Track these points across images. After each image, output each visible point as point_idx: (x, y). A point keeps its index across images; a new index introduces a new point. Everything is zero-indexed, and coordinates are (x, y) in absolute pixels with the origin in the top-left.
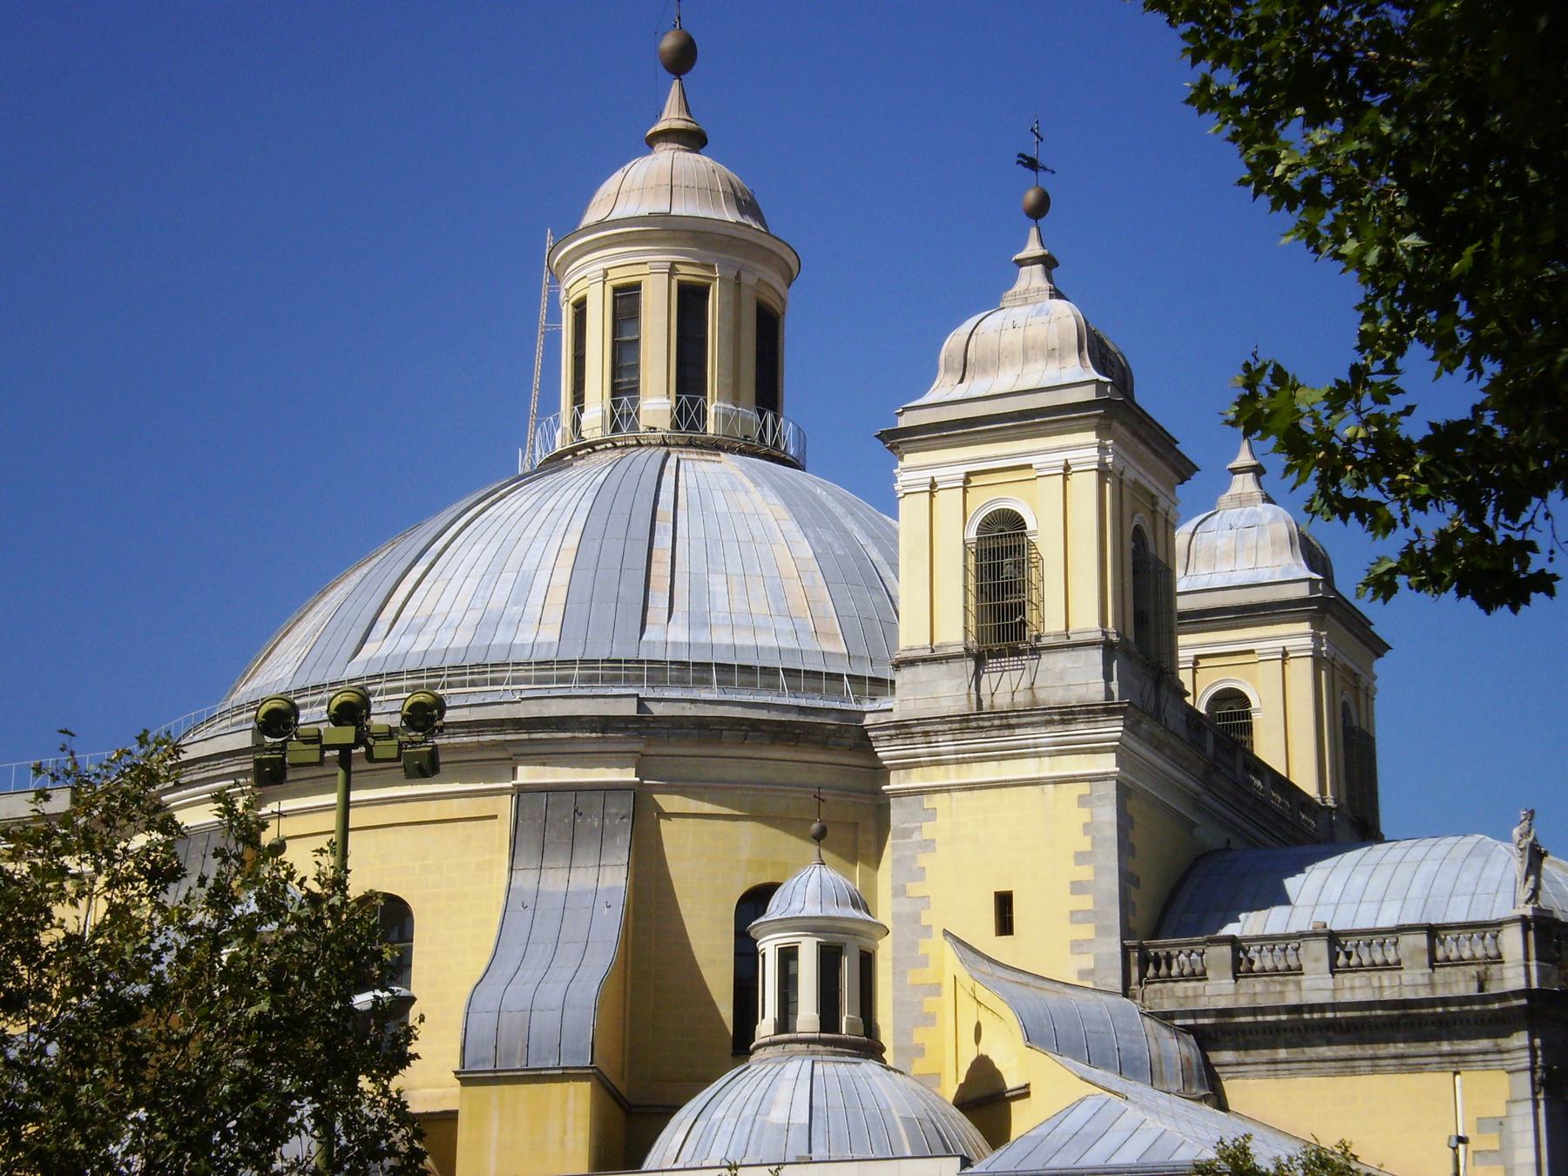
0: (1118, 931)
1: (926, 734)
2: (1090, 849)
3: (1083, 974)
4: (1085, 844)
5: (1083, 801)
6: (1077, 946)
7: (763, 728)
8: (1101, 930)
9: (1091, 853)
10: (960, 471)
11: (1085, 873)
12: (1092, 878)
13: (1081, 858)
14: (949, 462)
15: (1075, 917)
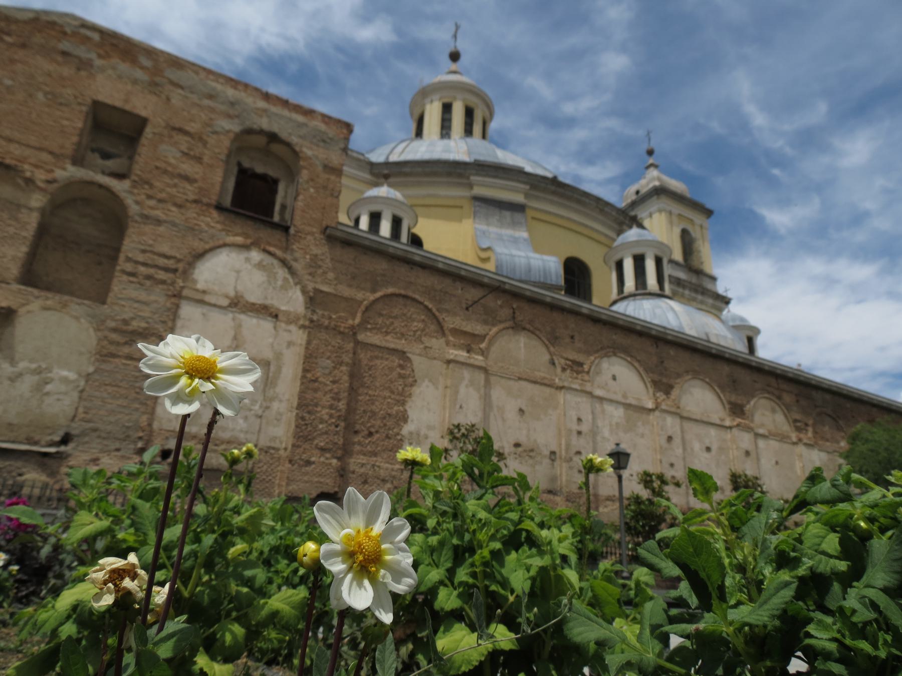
14: (677, 208)
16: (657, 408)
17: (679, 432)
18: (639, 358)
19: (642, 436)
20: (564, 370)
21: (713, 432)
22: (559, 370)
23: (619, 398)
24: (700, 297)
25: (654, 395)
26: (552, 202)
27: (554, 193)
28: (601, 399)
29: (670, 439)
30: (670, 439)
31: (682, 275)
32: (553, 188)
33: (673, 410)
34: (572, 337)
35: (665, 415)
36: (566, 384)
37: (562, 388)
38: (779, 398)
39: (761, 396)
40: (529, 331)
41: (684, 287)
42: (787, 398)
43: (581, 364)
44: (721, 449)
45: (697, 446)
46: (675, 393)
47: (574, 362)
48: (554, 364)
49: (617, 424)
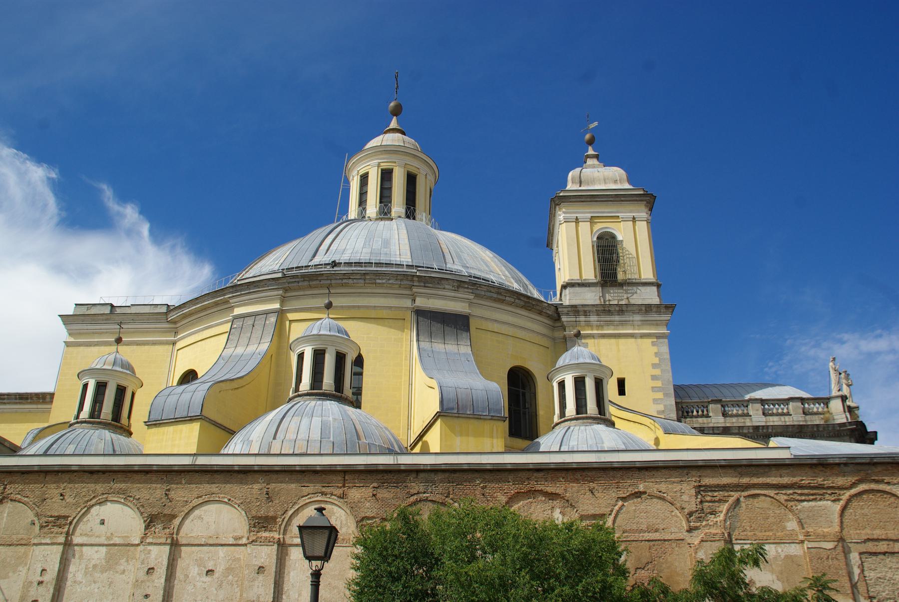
0: (673, 395)
1: (585, 312)
2: (658, 362)
3: (659, 412)
4: (656, 361)
5: (653, 344)
6: (655, 401)
7: (522, 298)
8: (666, 395)
9: (659, 364)
10: (589, 215)
11: (657, 372)
12: (660, 374)
13: (654, 366)
14: (585, 212)
15: (654, 389)
16: (142, 542)
17: (165, 562)
18: (137, 497)
19: (124, 572)
20: (42, 527)
21: (221, 551)
22: (37, 527)
23: (103, 540)
24: (617, 318)
25: (147, 528)
26: (314, 296)
27: (310, 287)
28: (82, 545)
29: (150, 570)
30: (150, 570)
31: (591, 297)
32: (306, 283)
33: (163, 540)
34: (62, 495)
35: (150, 547)
36: (36, 541)
37: (34, 544)
38: (342, 497)
39: (306, 500)
40: (15, 500)
41: (586, 313)
42: (355, 494)
43: (68, 517)
44: (229, 570)
45: (194, 571)
46: (177, 522)
47: (59, 517)
48: (34, 524)
49: (95, 566)
